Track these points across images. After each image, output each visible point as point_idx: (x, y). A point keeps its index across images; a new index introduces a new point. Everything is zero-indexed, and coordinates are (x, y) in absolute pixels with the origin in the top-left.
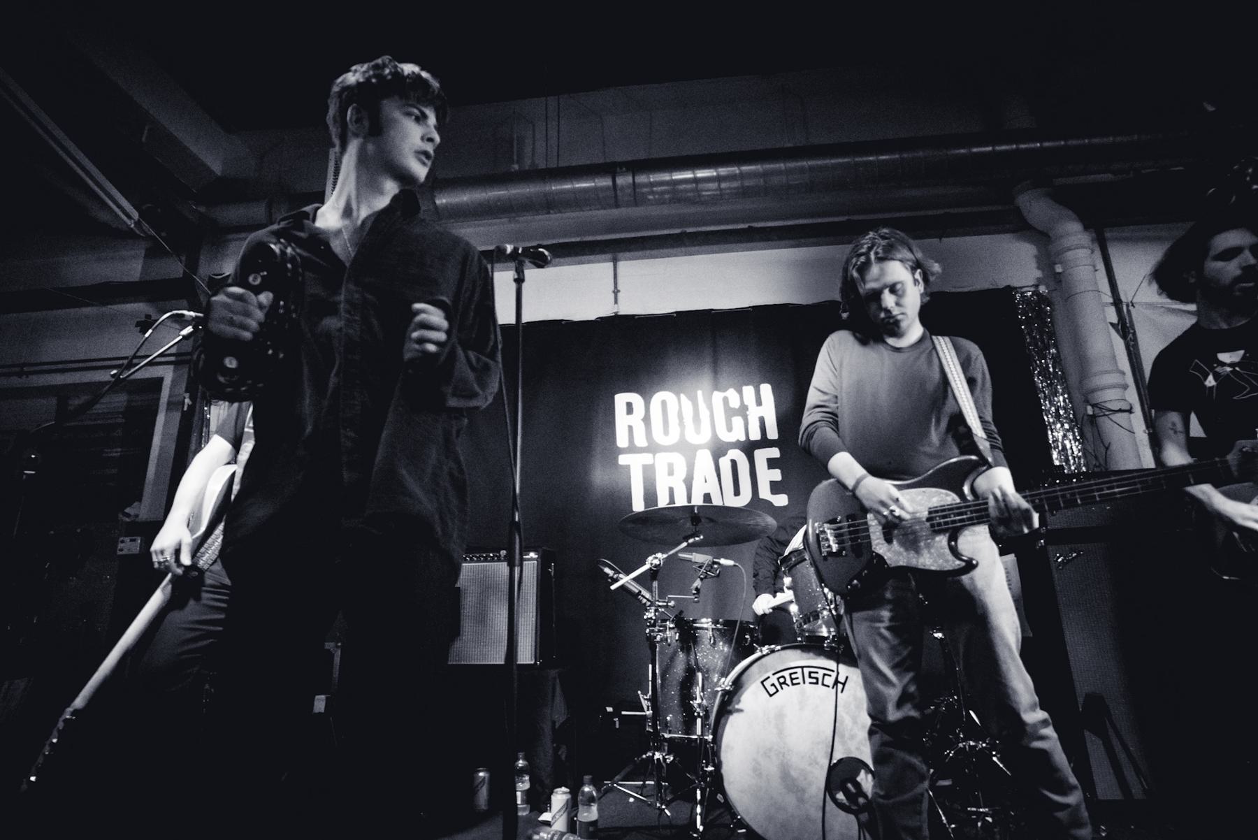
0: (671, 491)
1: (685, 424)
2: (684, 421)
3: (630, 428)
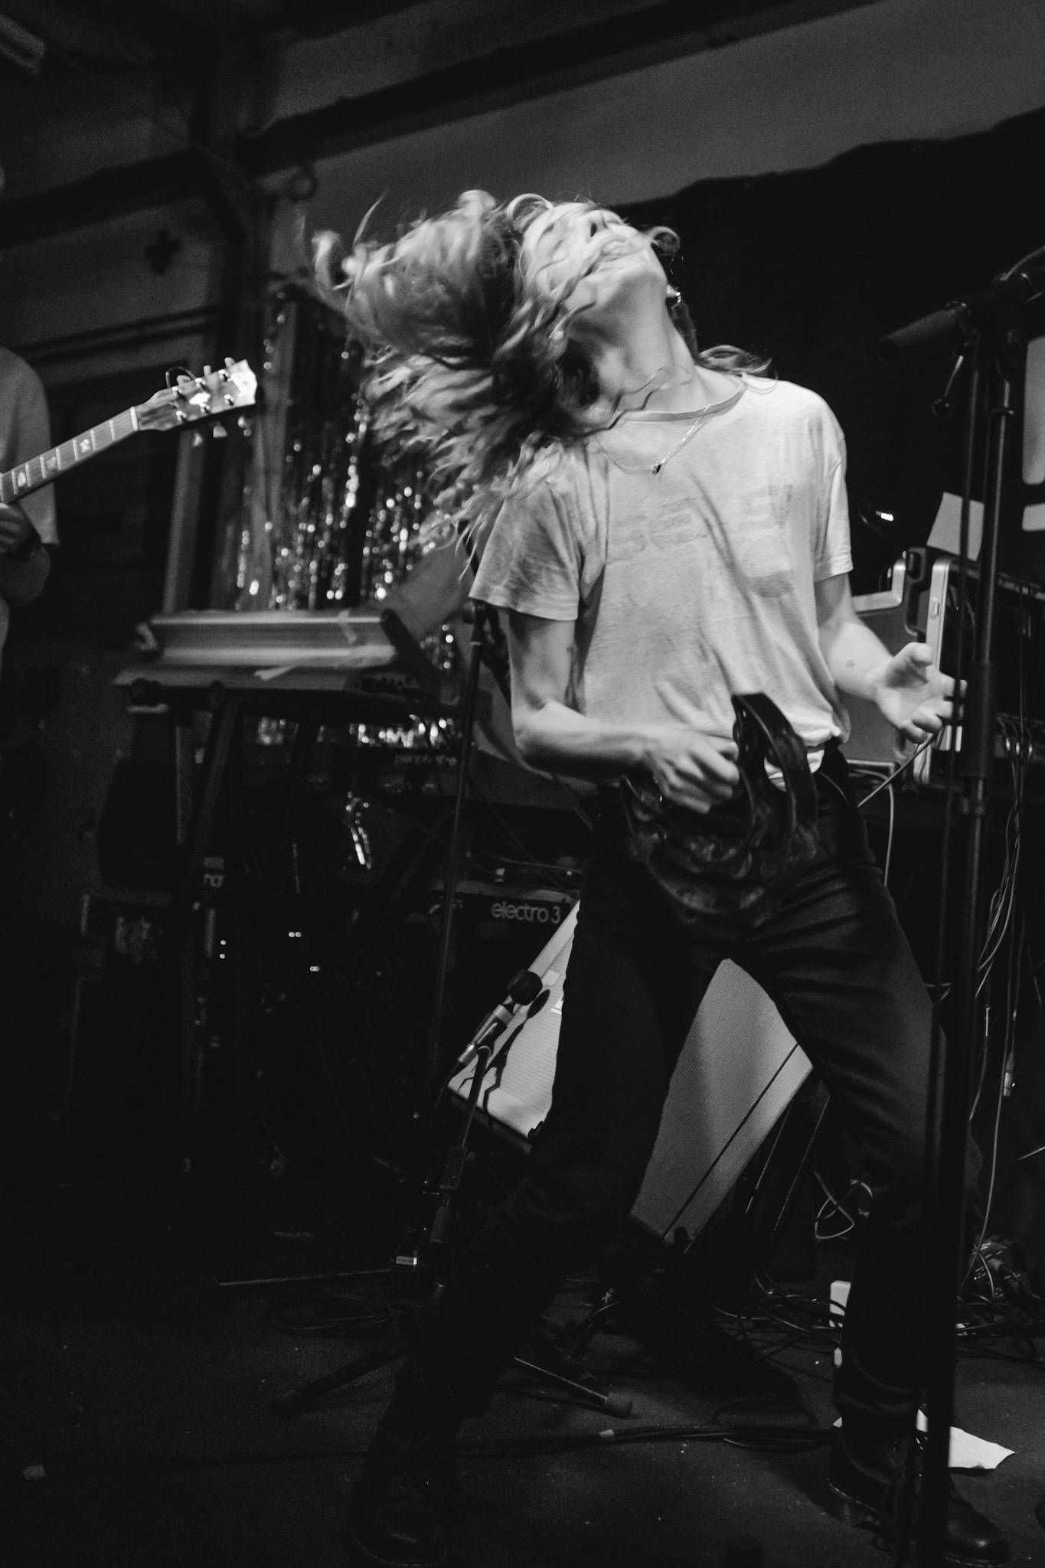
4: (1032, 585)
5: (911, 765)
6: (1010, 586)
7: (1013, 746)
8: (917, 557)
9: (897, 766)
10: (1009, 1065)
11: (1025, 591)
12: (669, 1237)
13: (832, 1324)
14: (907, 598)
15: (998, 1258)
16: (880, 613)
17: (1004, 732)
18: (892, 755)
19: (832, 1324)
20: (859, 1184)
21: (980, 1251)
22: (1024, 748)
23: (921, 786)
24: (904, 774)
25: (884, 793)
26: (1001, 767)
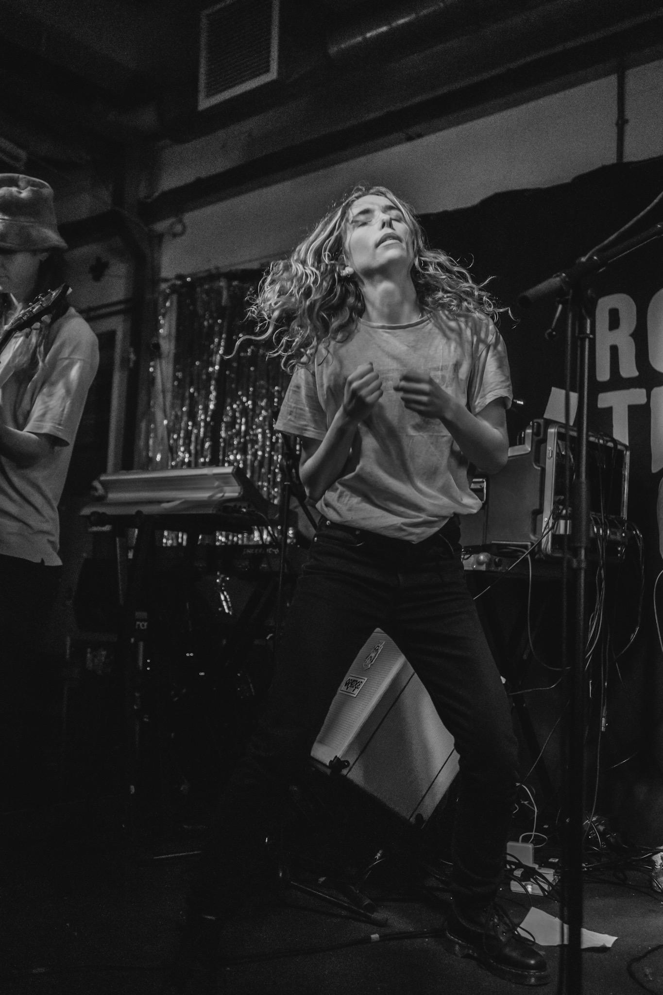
3: (614, 350)
4: (605, 438)
5: (540, 544)
6: (592, 439)
7: (598, 530)
8: (539, 424)
9: (532, 544)
10: (604, 712)
11: (601, 441)
12: (412, 820)
13: (508, 867)
14: (534, 448)
15: (602, 825)
16: (517, 457)
17: (593, 522)
18: (530, 539)
19: (508, 867)
20: (520, 787)
21: (592, 822)
22: (605, 531)
23: (547, 555)
24: (536, 549)
25: (525, 560)
26: (593, 541)
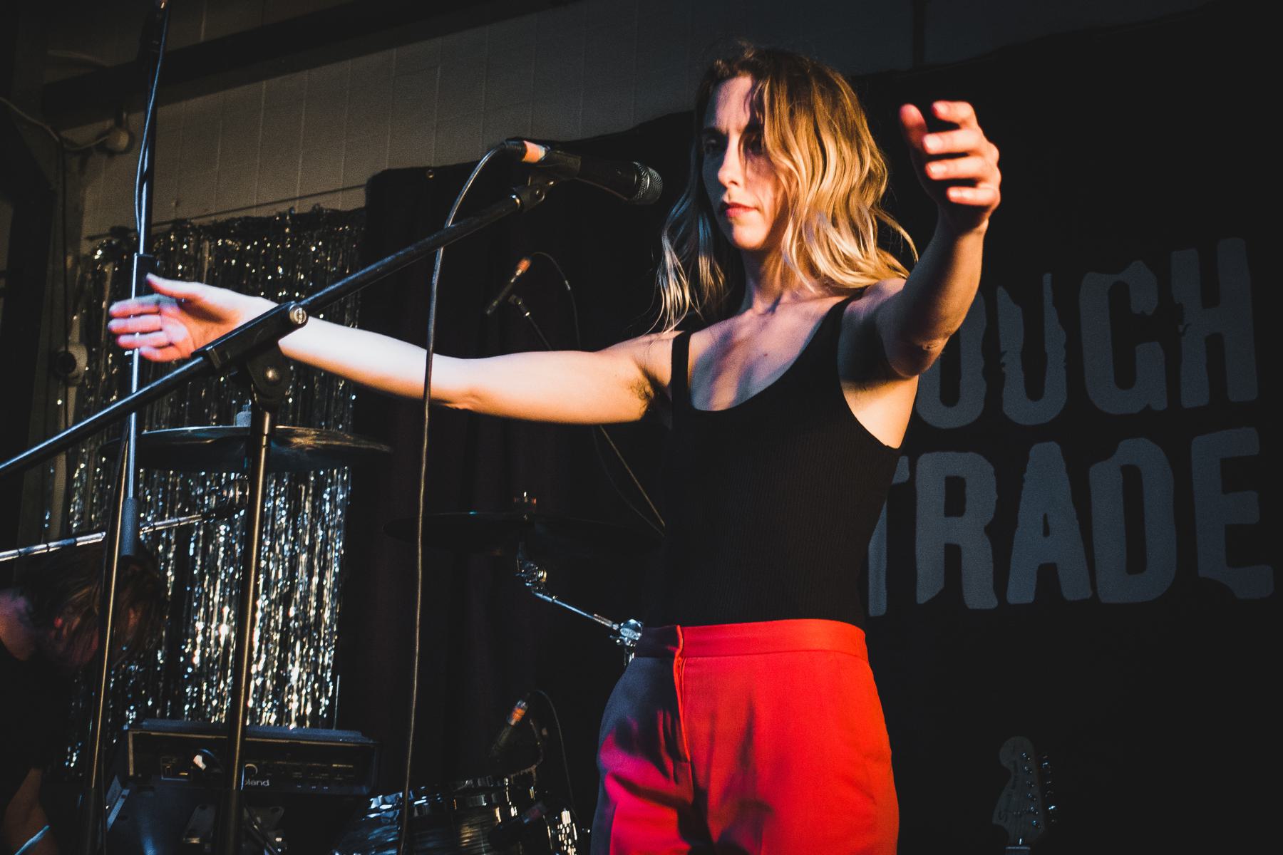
0: (953, 554)
1: (1004, 369)
2: (1003, 360)
